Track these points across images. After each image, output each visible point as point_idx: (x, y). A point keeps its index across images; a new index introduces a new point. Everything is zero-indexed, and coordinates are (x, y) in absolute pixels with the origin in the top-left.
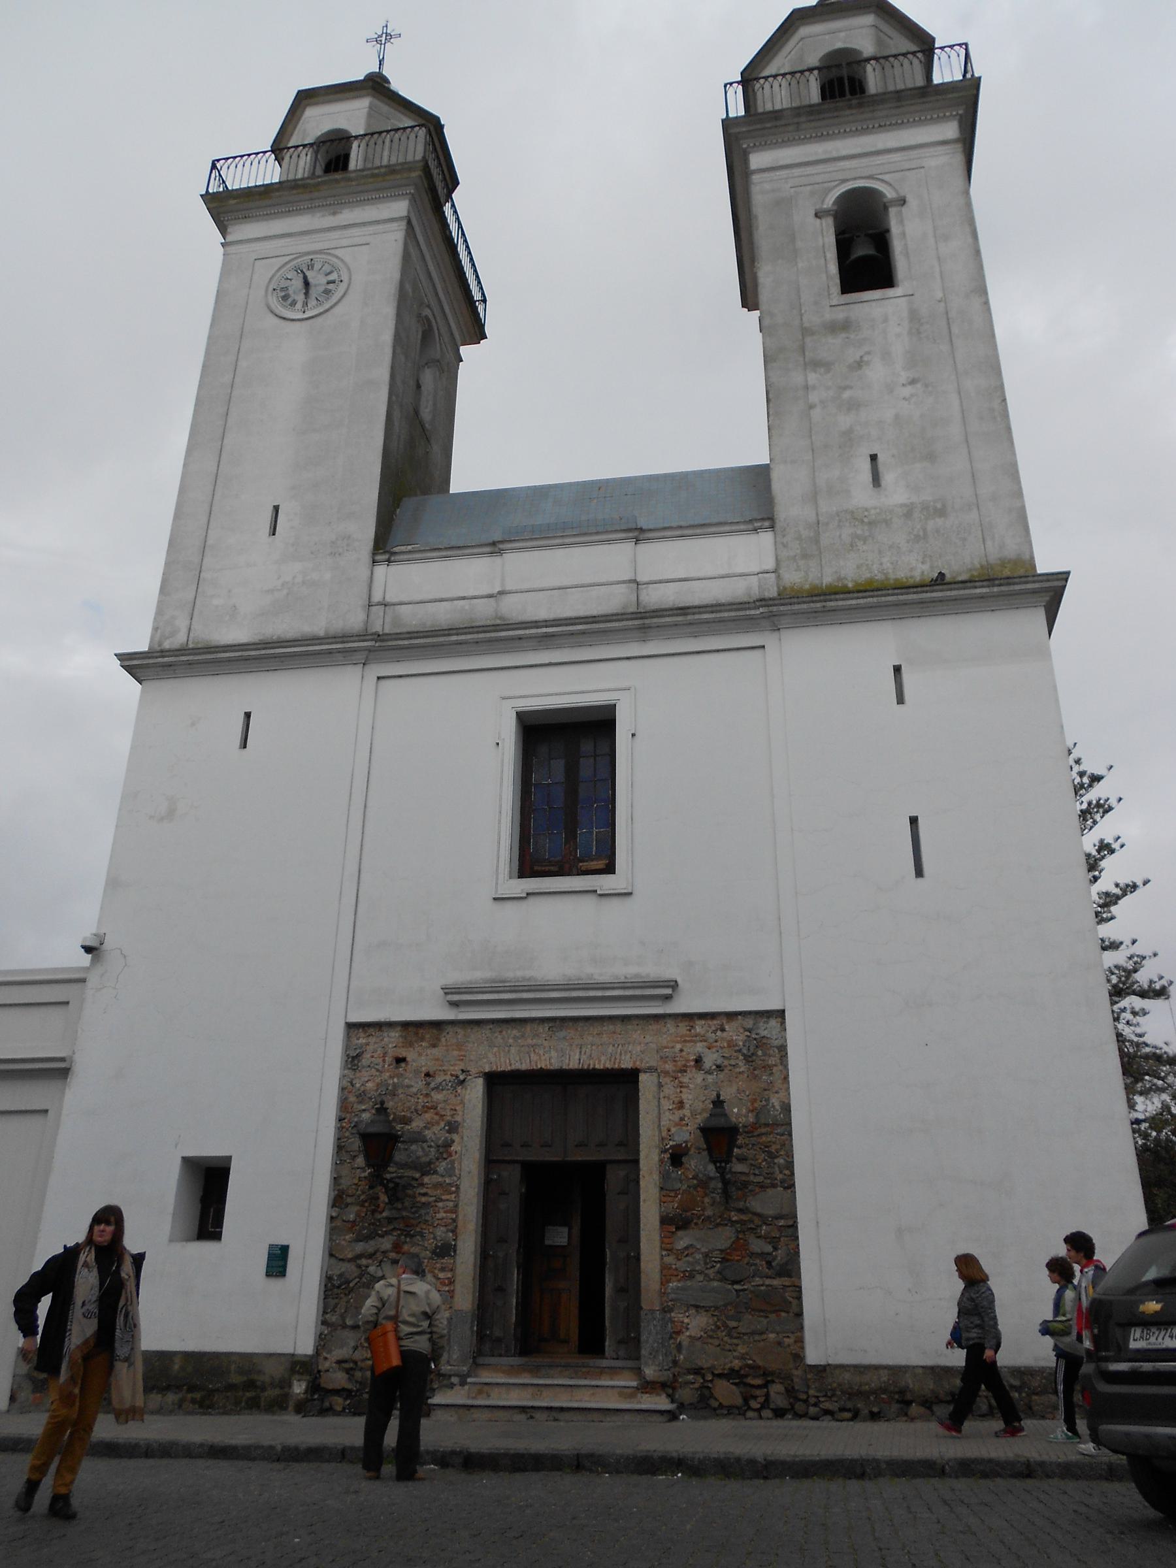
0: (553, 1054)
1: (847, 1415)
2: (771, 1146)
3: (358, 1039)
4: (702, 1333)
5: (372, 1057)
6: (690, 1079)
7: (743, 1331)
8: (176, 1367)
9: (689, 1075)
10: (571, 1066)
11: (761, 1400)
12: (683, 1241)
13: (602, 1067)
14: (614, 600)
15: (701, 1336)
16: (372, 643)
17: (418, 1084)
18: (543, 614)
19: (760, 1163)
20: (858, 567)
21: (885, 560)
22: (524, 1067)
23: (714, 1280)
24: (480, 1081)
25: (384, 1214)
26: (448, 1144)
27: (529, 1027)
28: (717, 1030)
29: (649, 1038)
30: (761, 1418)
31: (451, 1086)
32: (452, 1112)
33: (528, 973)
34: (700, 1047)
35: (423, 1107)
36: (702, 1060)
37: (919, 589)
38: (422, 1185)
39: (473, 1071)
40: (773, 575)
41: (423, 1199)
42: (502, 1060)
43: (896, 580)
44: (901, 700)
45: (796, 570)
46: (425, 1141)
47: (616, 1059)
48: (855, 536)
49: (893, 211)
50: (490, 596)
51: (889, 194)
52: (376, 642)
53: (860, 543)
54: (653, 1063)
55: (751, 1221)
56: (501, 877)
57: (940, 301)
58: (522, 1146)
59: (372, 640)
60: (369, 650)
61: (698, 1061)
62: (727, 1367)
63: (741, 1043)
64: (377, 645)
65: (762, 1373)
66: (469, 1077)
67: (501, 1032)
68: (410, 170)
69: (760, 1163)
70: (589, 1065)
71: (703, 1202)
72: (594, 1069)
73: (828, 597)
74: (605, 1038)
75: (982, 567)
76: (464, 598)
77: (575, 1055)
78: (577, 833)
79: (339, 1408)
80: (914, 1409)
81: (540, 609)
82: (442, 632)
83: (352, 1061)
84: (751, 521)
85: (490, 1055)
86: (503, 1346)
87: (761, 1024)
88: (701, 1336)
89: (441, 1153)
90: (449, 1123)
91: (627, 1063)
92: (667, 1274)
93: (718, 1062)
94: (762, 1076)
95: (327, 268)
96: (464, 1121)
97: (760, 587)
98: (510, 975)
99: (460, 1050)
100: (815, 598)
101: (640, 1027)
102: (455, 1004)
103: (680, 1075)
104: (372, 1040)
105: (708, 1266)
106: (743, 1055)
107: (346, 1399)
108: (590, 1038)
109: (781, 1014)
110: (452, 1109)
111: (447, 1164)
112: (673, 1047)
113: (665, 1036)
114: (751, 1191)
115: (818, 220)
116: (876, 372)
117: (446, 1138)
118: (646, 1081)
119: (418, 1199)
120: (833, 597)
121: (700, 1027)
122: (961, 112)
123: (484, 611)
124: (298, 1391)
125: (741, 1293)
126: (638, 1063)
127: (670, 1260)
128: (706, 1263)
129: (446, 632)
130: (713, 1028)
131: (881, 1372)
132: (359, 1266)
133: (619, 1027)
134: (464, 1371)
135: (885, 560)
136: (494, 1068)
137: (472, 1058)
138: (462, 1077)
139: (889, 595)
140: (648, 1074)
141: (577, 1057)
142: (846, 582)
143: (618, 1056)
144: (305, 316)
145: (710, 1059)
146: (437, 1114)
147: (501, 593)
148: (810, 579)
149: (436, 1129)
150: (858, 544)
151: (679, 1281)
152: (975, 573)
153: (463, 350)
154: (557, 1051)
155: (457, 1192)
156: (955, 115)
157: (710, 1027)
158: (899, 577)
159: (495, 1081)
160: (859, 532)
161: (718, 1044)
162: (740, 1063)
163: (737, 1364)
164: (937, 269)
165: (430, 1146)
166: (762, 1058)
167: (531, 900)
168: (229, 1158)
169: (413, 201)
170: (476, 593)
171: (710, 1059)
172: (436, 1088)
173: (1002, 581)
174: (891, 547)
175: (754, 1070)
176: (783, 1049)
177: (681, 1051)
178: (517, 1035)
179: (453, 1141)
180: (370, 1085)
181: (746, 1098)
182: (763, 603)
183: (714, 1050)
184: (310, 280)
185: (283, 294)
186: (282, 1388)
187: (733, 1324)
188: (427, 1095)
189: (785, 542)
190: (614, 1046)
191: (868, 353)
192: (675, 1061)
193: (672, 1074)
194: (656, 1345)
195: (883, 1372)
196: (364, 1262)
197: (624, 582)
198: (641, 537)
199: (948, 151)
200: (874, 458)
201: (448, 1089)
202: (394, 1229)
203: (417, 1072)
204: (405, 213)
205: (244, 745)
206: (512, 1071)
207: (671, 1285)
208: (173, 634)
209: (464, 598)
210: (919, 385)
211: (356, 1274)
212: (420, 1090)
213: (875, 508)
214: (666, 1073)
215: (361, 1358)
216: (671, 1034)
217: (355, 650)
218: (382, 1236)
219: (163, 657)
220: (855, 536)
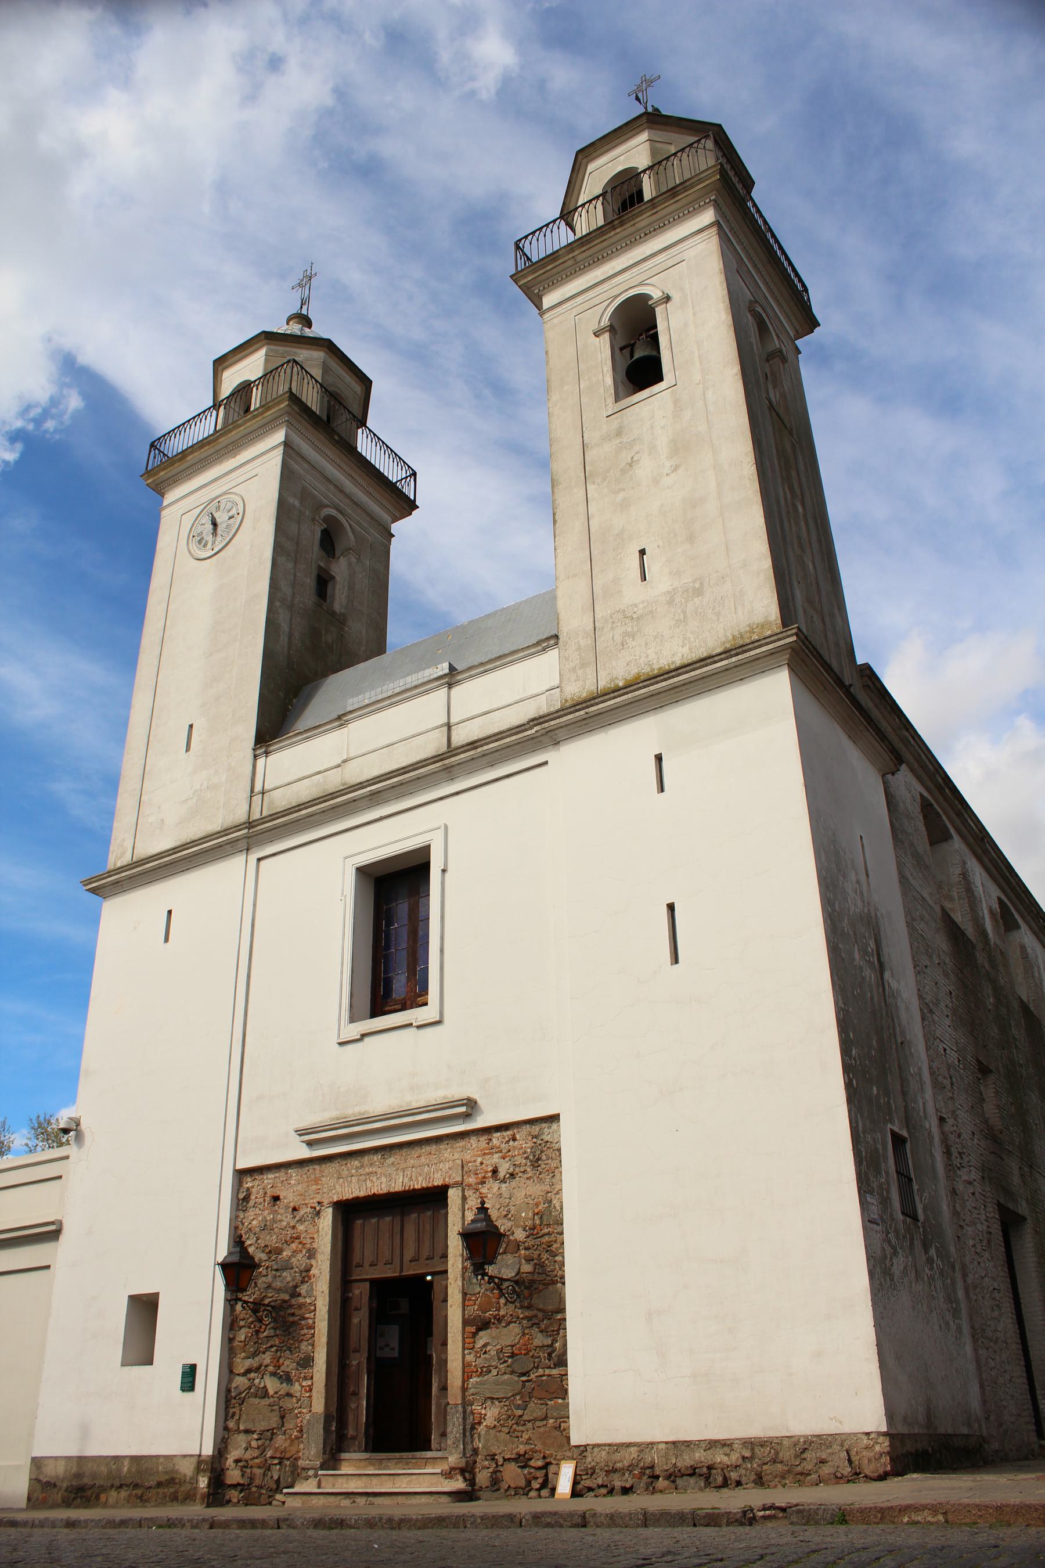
0: (384, 1179)
1: (604, 1491)
2: (552, 1245)
3: (247, 1183)
4: (496, 1423)
5: (256, 1198)
6: (488, 1189)
7: (528, 1419)
8: (126, 1469)
9: (487, 1186)
10: (396, 1190)
11: (540, 1480)
12: (483, 1338)
13: (419, 1187)
15: (495, 1425)
16: (246, 831)
17: (286, 1219)
19: (544, 1262)
20: (628, 664)
21: (650, 652)
22: (362, 1194)
23: (505, 1373)
24: (330, 1210)
25: (265, 1334)
26: (308, 1270)
27: (366, 1159)
28: (509, 1140)
29: (457, 1156)
30: (540, 1496)
31: (311, 1217)
32: (311, 1240)
34: (496, 1158)
35: (291, 1238)
36: (497, 1170)
37: (666, 676)
38: (291, 1306)
39: (326, 1202)
40: (558, 690)
41: (291, 1319)
42: (346, 1189)
43: (660, 669)
44: (661, 789)
45: (576, 681)
46: (292, 1268)
47: (430, 1178)
48: (626, 634)
49: (659, 311)
50: (339, 766)
51: (656, 294)
52: (249, 829)
53: (629, 640)
54: (459, 1179)
55: (536, 1316)
56: (342, 1022)
57: (698, 384)
58: (370, 1265)
59: (246, 828)
60: (247, 837)
61: (495, 1171)
62: (515, 1451)
63: (529, 1150)
64: (250, 831)
65: (542, 1456)
66: (323, 1208)
67: (346, 1164)
68: (280, 403)
69: (544, 1262)
70: (410, 1186)
71: (499, 1303)
72: (414, 1190)
73: (589, 703)
74: (423, 1159)
75: (734, 636)
76: (319, 773)
77: (399, 1178)
78: (416, 971)
79: (235, 1500)
80: (662, 1483)
82: (294, 809)
83: (241, 1202)
84: (538, 643)
85: (337, 1187)
86: (357, 1443)
87: (546, 1129)
88: (495, 1425)
89: (304, 1277)
90: (309, 1250)
91: (438, 1182)
92: (467, 1373)
93: (511, 1170)
94: (545, 1179)
95: (230, 505)
96: (319, 1247)
97: (547, 703)
98: (350, 1112)
99: (317, 1184)
100: (577, 707)
101: (450, 1145)
102: (310, 1144)
103: (480, 1186)
104: (256, 1183)
105: (501, 1361)
106: (531, 1161)
107: (241, 1492)
108: (412, 1162)
109: (554, 1118)
110: (311, 1238)
111: (308, 1287)
112: (475, 1161)
113: (469, 1151)
114: (536, 1289)
115: (598, 339)
116: (645, 469)
117: (306, 1264)
118: (454, 1195)
119: (287, 1319)
120: (592, 702)
121: (497, 1138)
122: (714, 197)
123: (334, 781)
124: (202, 1486)
125: (527, 1384)
126: (447, 1180)
127: (470, 1358)
128: (499, 1359)
129: (297, 808)
130: (507, 1139)
131: (632, 1449)
133: (433, 1148)
134: (317, 1465)
135: (650, 652)
136: (341, 1198)
137: (325, 1190)
138: (318, 1208)
139: (640, 688)
140: (454, 1189)
141: (401, 1180)
142: (617, 682)
143: (432, 1175)
144: (214, 552)
145: (504, 1169)
146: (300, 1243)
147: (344, 761)
148: (587, 687)
149: (299, 1256)
150: (628, 641)
151: (479, 1376)
152: (728, 646)
153: (396, 528)
154: (385, 1176)
155: (315, 1310)
156: (708, 203)
157: (504, 1138)
158: (663, 665)
160: (629, 629)
161: (510, 1153)
162: (528, 1170)
163: (522, 1449)
164: (696, 354)
165: (295, 1272)
166: (546, 1162)
167: (367, 1039)
168: (157, 1294)
169: (289, 424)
170: (329, 766)
171: (504, 1169)
172: (299, 1221)
173: (738, 651)
174: (656, 637)
175: (540, 1174)
177: (482, 1163)
178: (359, 1165)
179: (312, 1266)
180: (254, 1222)
181: (531, 1202)
182: (536, 722)
183: (507, 1159)
184: (218, 521)
185: (199, 538)
186: (192, 1484)
187: (519, 1412)
188: (294, 1227)
189: (567, 655)
190: (428, 1166)
191: (638, 453)
192: (476, 1174)
193: (474, 1186)
194: (458, 1435)
195: (633, 1449)
197: (437, 728)
198: (453, 681)
199: (705, 238)
200: (642, 552)
201: (309, 1220)
202: (272, 1346)
204: (283, 439)
205: (167, 940)
206: (353, 1199)
207: (471, 1380)
208: (124, 853)
209: (319, 773)
210: (680, 471)
211: (247, 1386)
212: (288, 1223)
213: (643, 602)
214: (470, 1185)
215: (250, 1457)
216: (474, 1149)
217: (237, 840)
218: (264, 1353)
219: (110, 876)
220: (626, 634)
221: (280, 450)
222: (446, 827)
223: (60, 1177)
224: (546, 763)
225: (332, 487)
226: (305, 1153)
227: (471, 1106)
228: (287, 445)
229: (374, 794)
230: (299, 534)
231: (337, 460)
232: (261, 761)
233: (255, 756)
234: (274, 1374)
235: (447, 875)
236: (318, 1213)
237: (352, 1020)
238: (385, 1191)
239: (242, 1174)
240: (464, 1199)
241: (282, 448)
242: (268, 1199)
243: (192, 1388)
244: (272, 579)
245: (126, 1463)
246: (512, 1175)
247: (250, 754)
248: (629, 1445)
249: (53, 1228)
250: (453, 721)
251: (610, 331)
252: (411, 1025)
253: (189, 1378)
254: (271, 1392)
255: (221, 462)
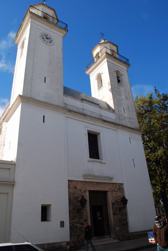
22: (94, 190)
24: (88, 192)
34: (114, 188)
39: (87, 190)
54: (110, 190)
61: (114, 190)
91: (107, 190)
102: (84, 178)
132: (73, 224)
159: (90, 192)
171: (116, 190)
176: (123, 189)
188: (80, 194)
196: (73, 223)
203: (78, 189)
226: (83, 180)
227: (111, 179)
234: (79, 223)
236: (85, 192)
238: (98, 190)
239: (69, 181)
242: (74, 187)
243: (63, 226)
245: (51, 245)
246: (117, 191)
248: (137, 232)
253: (62, 224)
254: (78, 227)
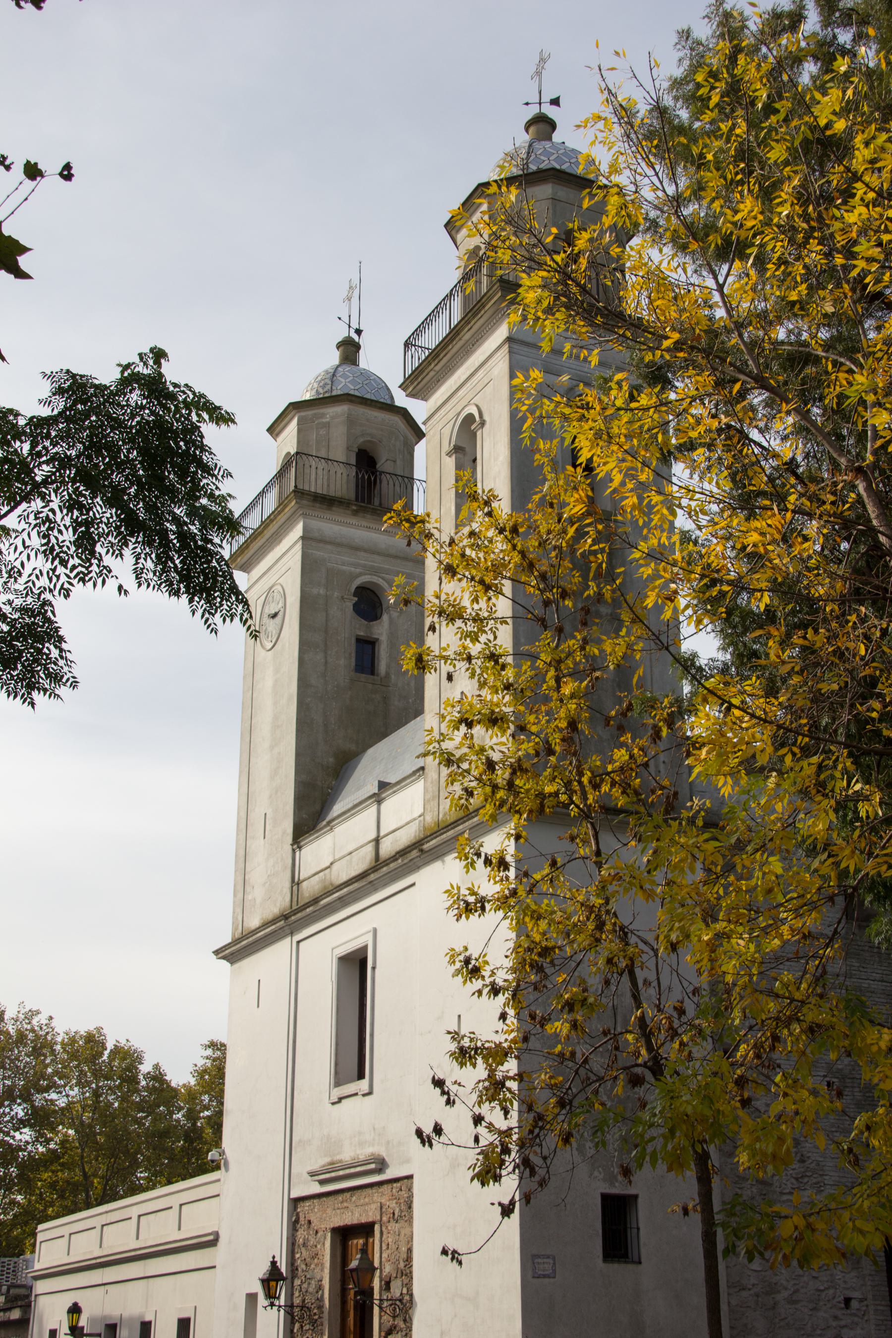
14: (361, 862)
18: (344, 877)
27: (340, 1198)
33: (338, 1157)
68: (290, 501)
81: (343, 872)
83: (294, 1225)
91: (370, 1220)
109: (410, 1177)
118: (377, 1228)
133: (369, 1191)
169: (304, 515)
221: (299, 546)
222: (375, 931)
223: (218, 1195)
224: (413, 884)
225: (362, 554)
227: (381, 1165)
228: (305, 538)
229: (340, 898)
230: (327, 621)
231: (365, 523)
232: (297, 853)
233: (294, 850)
235: (377, 970)
237: (338, 1083)
239: (296, 1202)
240: (382, 1233)
241: (300, 543)
244: (300, 679)
247: (289, 848)
249: (211, 1237)
250: (382, 834)
251: (456, 452)
252: (356, 1094)
255: (280, 541)
